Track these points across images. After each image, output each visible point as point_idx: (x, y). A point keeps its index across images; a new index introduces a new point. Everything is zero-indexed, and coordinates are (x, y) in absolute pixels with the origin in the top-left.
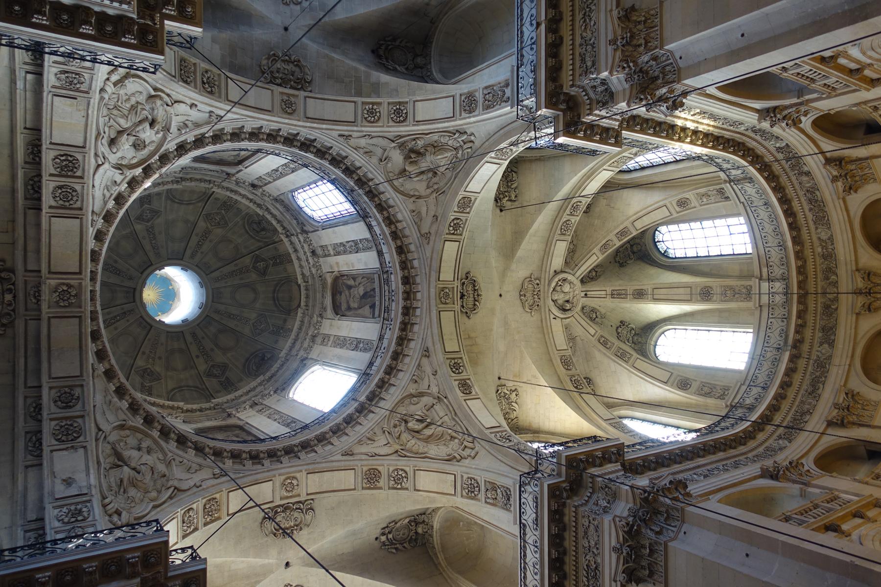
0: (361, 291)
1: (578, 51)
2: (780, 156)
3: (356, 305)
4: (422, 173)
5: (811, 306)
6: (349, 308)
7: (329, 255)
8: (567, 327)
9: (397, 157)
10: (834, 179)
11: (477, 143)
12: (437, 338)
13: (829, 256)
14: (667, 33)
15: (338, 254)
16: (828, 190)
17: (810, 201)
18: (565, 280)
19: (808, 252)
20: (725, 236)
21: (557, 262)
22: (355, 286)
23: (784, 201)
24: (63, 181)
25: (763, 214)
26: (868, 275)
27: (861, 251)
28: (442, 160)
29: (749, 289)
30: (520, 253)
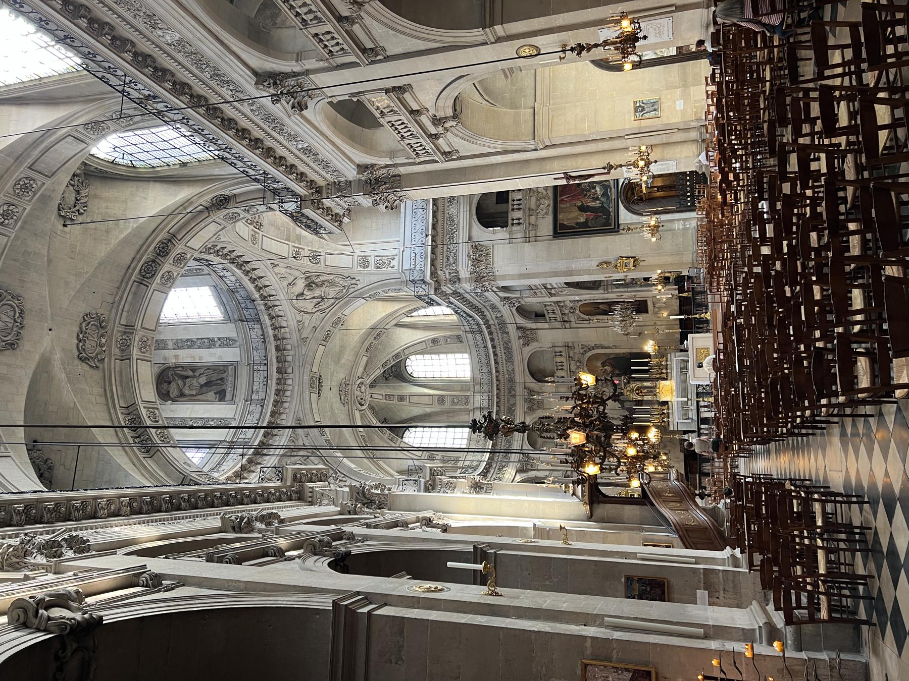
0: (203, 380)
1: (445, 254)
2: (496, 322)
3: (194, 393)
4: (314, 298)
5: (502, 408)
6: (182, 395)
7: (164, 348)
8: (361, 417)
9: (300, 285)
10: (520, 338)
11: (359, 287)
12: (308, 411)
13: (512, 380)
14: (495, 260)
15: (179, 348)
16: (516, 343)
17: (505, 348)
18: (362, 383)
19: (501, 377)
20: (456, 366)
21: (361, 369)
22: (195, 377)
23: (494, 347)
24: (172, 268)
25: (482, 352)
26: (531, 392)
27: (527, 378)
28: (332, 292)
29: (467, 397)
30: (343, 361)
